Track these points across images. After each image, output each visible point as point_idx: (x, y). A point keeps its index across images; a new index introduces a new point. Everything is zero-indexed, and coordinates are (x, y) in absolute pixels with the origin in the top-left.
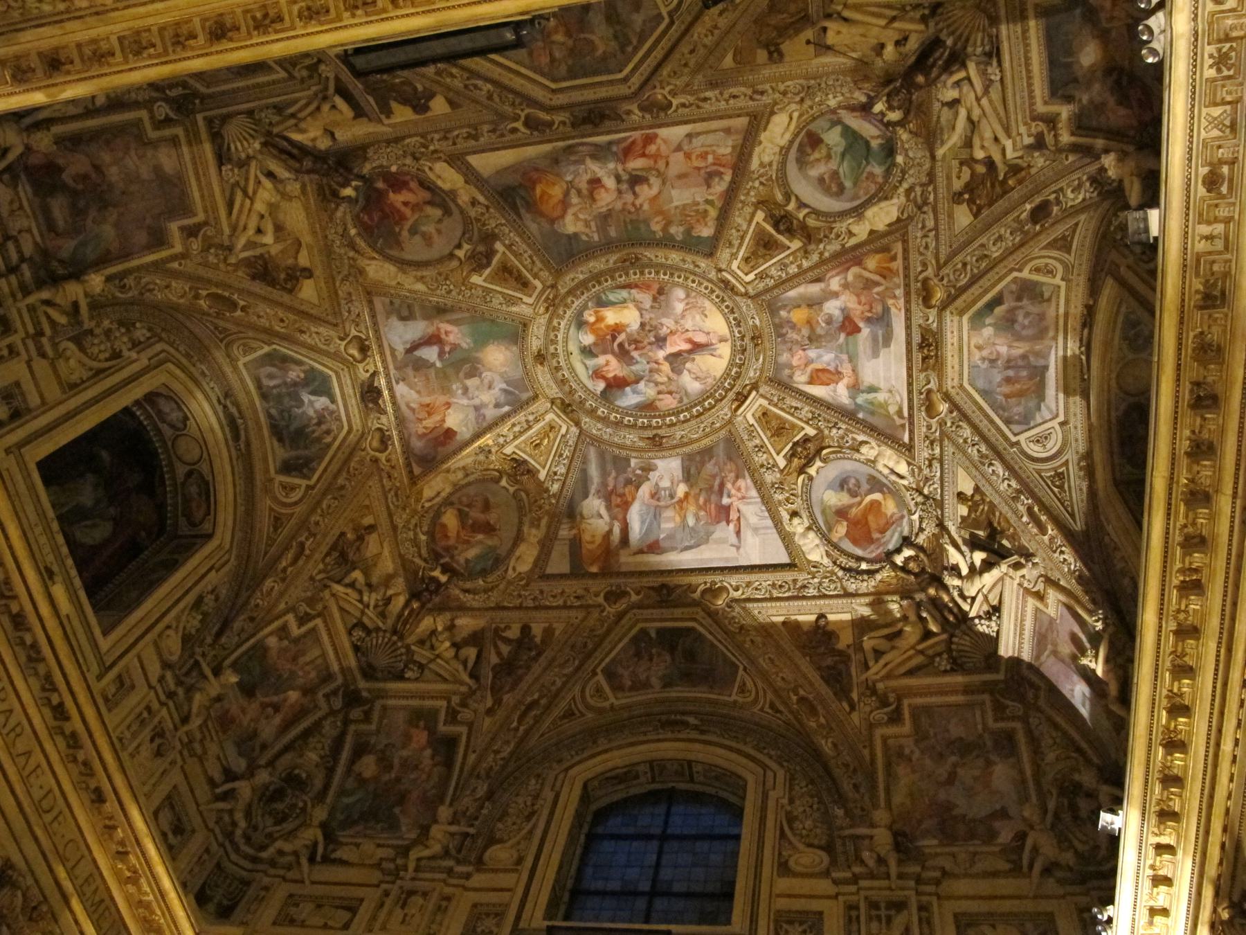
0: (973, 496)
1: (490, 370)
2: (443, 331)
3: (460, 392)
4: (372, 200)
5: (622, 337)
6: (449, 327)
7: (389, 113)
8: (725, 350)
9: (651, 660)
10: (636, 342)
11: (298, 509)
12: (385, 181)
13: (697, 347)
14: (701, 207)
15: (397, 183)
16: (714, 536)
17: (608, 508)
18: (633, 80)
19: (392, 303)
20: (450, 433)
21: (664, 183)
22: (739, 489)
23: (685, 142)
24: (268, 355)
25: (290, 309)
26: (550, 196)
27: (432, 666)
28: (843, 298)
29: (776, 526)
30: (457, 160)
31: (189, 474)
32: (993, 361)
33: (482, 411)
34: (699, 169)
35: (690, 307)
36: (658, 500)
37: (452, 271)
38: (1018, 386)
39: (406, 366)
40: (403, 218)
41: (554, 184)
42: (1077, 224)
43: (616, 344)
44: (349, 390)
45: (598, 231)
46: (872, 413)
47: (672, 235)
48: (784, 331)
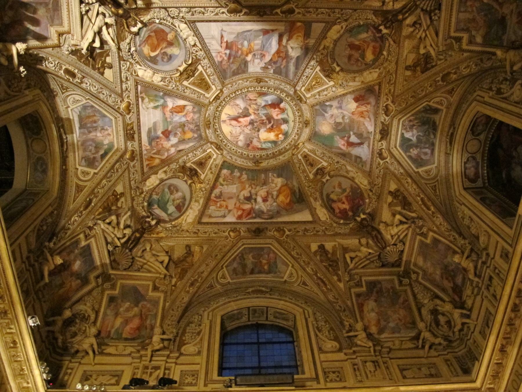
0: (104, 69)
1: (330, 123)
3: (346, 118)
4: (356, 208)
5: (269, 126)
6: (342, 147)
7: (334, 247)
8: (224, 117)
10: (263, 123)
11: (438, 95)
12: (348, 215)
13: (236, 119)
14: (225, 183)
15: (344, 214)
16: (234, 36)
17: (287, 51)
18: (240, 245)
19: (362, 166)
20: (356, 100)
21: (238, 196)
22: (221, 56)
23: (226, 214)
24: (421, 166)
25: (403, 185)
26: (284, 196)
28: (169, 145)
29: (203, 40)
30: (316, 220)
31: (479, 134)
32: (103, 129)
33: (338, 105)
34: (224, 201)
35: (237, 137)
36: (261, 54)
37: (334, 171)
38: (91, 120)
39: (366, 138)
40: (347, 197)
41: (281, 202)
42: (74, 201)
43: (272, 124)
44: (393, 138)
45: (269, 177)
46: (156, 96)
47: (239, 172)
48: (196, 128)
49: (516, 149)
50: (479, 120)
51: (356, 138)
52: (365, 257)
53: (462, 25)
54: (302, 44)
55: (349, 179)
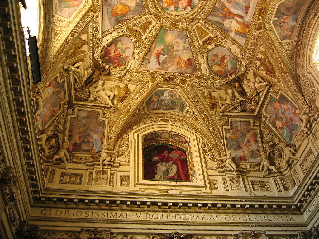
2: (156, 52)
3: (177, 52)
6: (156, 50)
7: (84, 52)
9: (285, 23)
17: (229, 18)
20: (189, 60)
26: (121, 9)
27: (258, 92)
30: (103, 34)
31: (172, 137)
33: (185, 48)
36: (232, 1)
37: (139, 43)
39: (163, 66)
41: (118, 7)
49: (173, 163)
50: (182, 138)
51: (162, 60)
52: (80, 76)
53: (234, 124)
54: (232, 29)
55: (133, 55)
